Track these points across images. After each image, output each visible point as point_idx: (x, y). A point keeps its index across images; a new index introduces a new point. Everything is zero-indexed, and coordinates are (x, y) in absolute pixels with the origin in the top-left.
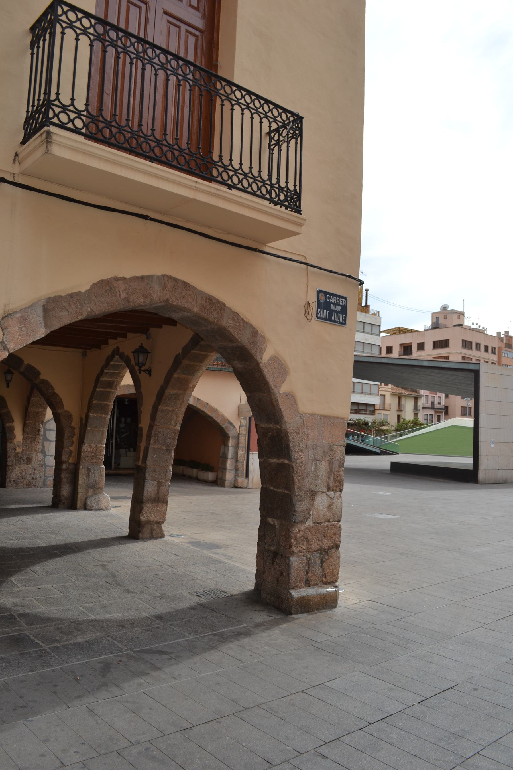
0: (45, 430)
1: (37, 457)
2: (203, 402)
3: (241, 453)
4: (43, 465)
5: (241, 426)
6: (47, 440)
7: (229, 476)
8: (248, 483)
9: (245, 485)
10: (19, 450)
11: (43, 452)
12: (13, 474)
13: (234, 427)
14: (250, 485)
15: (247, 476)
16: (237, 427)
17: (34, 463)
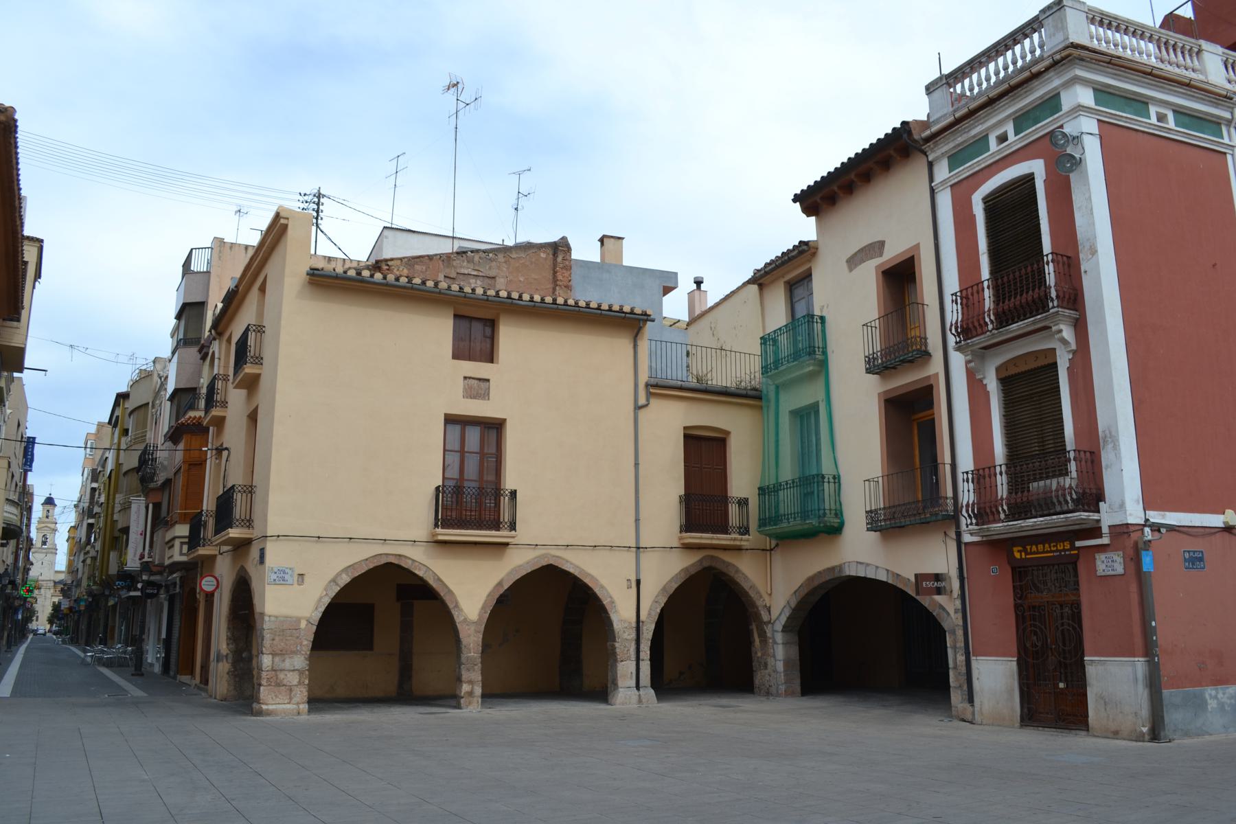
0: (774, 631)
1: (771, 661)
2: (904, 578)
3: (961, 658)
4: (775, 671)
5: (956, 611)
6: (775, 642)
7: (956, 697)
8: (973, 713)
9: (969, 717)
10: (759, 654)
11: (774, 656)
12: (757, 682)
13: (948, 614)
14: (978, 718)
15: (971, 700)
16: (952, 612)
17: (770, 669)
